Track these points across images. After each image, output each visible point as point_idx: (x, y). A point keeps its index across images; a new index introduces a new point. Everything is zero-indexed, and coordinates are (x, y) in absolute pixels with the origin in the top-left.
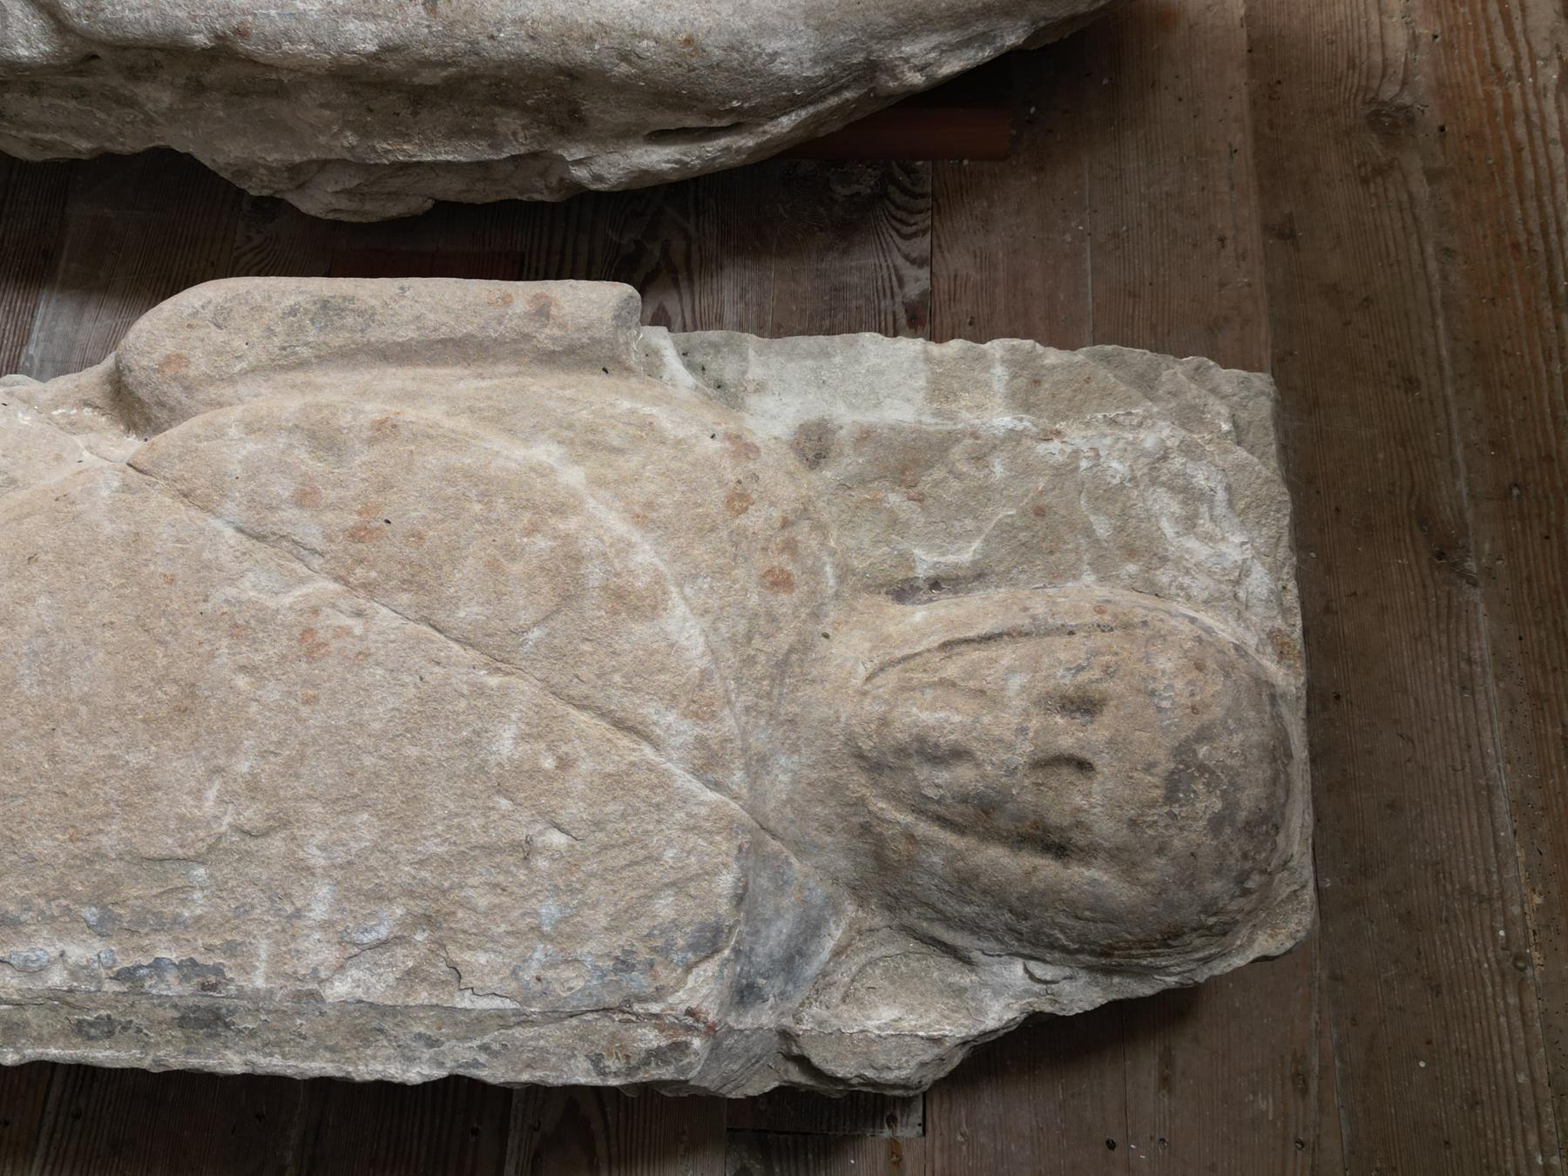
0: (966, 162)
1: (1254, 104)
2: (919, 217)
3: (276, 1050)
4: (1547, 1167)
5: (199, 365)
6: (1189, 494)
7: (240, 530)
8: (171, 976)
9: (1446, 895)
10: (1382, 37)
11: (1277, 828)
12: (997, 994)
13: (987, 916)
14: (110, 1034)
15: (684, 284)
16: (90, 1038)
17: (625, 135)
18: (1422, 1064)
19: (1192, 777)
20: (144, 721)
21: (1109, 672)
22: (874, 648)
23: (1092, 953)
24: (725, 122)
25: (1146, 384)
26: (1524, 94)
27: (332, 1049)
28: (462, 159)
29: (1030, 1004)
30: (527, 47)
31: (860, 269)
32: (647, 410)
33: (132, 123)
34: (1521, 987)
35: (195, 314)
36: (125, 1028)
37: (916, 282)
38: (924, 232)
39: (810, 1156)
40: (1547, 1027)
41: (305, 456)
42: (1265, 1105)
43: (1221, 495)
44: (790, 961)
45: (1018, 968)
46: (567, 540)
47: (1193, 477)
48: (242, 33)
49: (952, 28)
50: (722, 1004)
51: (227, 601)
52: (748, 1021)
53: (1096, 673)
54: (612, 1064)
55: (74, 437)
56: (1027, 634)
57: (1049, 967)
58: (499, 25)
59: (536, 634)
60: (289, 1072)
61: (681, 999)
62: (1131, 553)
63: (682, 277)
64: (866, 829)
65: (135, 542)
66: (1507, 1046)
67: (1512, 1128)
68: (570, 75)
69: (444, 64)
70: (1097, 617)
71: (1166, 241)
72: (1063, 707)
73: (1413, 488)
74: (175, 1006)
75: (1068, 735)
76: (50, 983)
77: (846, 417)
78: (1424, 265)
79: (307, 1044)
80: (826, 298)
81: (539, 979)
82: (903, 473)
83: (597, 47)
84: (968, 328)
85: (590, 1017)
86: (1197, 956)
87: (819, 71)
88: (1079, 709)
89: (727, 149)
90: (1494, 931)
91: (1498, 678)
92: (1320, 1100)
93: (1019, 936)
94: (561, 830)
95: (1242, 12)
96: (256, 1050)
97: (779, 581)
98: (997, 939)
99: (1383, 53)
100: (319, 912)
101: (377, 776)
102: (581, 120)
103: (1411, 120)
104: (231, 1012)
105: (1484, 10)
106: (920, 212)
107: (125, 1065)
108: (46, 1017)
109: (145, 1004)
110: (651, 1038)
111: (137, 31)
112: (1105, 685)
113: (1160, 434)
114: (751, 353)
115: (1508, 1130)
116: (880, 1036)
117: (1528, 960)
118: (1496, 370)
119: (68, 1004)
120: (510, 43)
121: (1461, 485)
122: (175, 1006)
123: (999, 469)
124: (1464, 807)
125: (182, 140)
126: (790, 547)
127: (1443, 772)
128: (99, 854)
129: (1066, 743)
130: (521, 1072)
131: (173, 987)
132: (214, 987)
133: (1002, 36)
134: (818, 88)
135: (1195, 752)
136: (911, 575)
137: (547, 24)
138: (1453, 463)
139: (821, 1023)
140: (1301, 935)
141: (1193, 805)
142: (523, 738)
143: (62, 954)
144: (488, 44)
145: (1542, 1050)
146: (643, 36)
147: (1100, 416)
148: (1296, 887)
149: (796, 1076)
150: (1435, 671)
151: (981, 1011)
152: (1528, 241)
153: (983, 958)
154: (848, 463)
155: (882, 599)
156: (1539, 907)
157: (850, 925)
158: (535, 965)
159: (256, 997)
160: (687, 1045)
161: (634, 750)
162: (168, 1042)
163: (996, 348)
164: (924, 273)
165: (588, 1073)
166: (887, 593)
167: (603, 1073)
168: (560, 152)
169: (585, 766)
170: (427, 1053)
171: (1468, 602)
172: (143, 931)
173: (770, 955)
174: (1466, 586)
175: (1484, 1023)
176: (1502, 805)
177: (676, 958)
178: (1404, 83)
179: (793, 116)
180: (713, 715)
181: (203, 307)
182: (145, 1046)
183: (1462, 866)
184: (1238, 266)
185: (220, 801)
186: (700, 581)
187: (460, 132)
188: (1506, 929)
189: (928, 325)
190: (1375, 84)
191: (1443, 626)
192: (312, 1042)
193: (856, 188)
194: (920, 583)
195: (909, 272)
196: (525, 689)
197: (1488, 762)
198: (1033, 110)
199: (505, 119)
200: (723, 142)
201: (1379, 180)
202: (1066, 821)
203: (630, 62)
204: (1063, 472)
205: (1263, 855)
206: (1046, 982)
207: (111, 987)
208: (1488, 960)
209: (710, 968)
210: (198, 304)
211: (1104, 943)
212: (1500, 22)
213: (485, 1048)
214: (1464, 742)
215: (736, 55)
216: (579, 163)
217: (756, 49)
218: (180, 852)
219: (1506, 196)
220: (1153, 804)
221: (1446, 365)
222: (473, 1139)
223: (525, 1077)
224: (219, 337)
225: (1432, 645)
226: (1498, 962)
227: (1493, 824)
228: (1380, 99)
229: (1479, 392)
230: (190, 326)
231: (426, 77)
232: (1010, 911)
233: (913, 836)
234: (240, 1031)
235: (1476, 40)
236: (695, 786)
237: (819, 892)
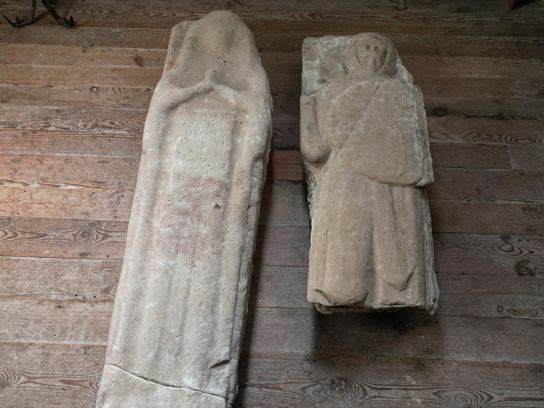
5: (320, 145)
6: (328, 44)
21: (363, 44)
22: (359, 70)
32: (324, 92)
46: (350, 95)
53: (363, 46)
59: (365, 97)
65: (354, 143)
70: (353, 48)
77: (318, 78)
93: (394, 62)
100: (407, 119)
110: (416, 89)
113: (319, 46)
123: (326, 62)
128: (403, 142)
129: (373, 49)
131: (419, 135)
142: (381, 98)
154: (326, 77)
163: (304, 62)
169: (384, 92)
185: (393, 130)
196: (373, 98)
204: (326, 55)
207: (420, 142)
224: (314, 142)
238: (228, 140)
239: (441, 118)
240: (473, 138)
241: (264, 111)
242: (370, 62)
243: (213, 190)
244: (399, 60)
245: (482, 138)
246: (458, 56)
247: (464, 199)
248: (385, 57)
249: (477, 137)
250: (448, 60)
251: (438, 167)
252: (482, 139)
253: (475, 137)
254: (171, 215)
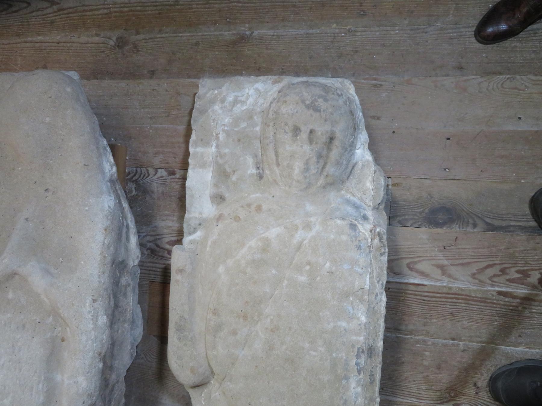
0: (127, 158)
1: (113, 79)
2: (143, 171)
3: (378, 334)
4: (398, 30)
6: (236, 101)
7: (243, 349)
8: (359, 361)
9: (333, 47)
10: (95, 43)
11: (326, 86)
12: (364, 157)
13: (346, 158)
14: (373, 375)
15: (160, 237)
16: (374, 380)
17: (127, 249)
18: (375, 56)
19: (315, 105)
20: (295, 371)
21: (286, 124)
23: (355, 132)
24: (125, 222)
25: (203, 112)
26: (115, 8)
27: (378, 320)
28: (132, 294)
29: (366, 149)
30: (106, 275)
31: (158, 188)
33: (118, 387)
34: (355, 31)
35: (179, 366)
36: (372, 371)
37: (162, 172)
38: (147, 170)
39: (396, 206)
40: (366, 27)
41: (222, 334)
42: (384, 94)
43: (236, 94)
44: (357, 207)
45: (357, 151)
47: (230, 101)
48: (100, 354)
49: (102, 158)
50: (368, 224)
51: (263, 351)
52: (371, 218)
54: (383, 250)
55: (212, 397)
56: (275, 144)
57: (358, 143)
58: (100, 282)
60: (383, 330)
61: (368, 234)
62: (251, 118)
63: (158, 237)
64: (324, 187)
66: (370, 36)
67: (390, 37)
68: (113, 263)
69: (110, 298)
71: (153, 105)
72: (295, 136)
73: (226, 45)
74: (367, 359)
75: (304, 136)
76: (361, 391)
78: (164, 37)
79: (376, 325)
80: (166, 197)
81: (362, 269)
82: (227, 176)
83: (107, 255)
84: (176, 159)
85: (371, 256)
86: (355, 107)
87: (112, 195)
88: (296, 132)
89: (131, 221)
90: (342, 36)
91: (278, 29)
92: (383, 81)
94: (326, 263)
95: (85, 81)
96: (378, 339)
97: (259, 209)
98: (351, 156)
99: (100, 43)
101: (311, 311)
102: (123, 261)
103: (121, 38)
104: (369, 345)
105: (89, 16)
106: (141, 171)
107: (380, 371)
108: (369, 392)
109: (366, 367)
110: (376, 241)
111: (98, 384)
112: (290, 125)
114: (190, 216)
115: (390, 38)
116: (374, 186)
117: (349, 29)
118: (194, 22)
119: (366, 386)
120: (105, 279)
121: (226, 33)
122: (367, 359)
123: (227, 151)
124: (311, 41)
125: (123, 372)
126: (249, 205)
127: (302, 45)
130: (384, 273)
131: (363, 360)
132: (363, 350)
133: (104, 145)
134: (116, 196)
135: (308, 104)
136: (256, 174)
137: (100, 269)
138: (220, 35)
139: (371, 200)
140: (350, 82)
141: (321, 105)
143: (354, 388)
144: (105, 285)
145: (371, 28)
146: (104, 243)
147: (213, 124)
148: (338, 83)
149: (382, 207)
150: (276, 44)
151: (368, 161)
152: (158, 10)
153: (355, 160)
154: (223, 190)
155: (262, 181)
156: (337, 25)
157: (347, 192)
158: (359, 270)
159: (367, 339)
160: (378, 232)
161: (305, 245)
162: (375, 360)
163: (191, 150)
164: (159, 170)
165: (385, 257)
166: (260, 181)
167: (385, 253)
168: (131, 268)
170: (379, 296)
171: (258, 34)
172: (349, 368)
173: (356, 212)
174: (254, 34)
175: (365, 41)
176: (311, 31)
177: (358, 234)
178: (110, 39)
179: (123, 203)
180: (296, 225)
181: (177, 363)
182: (377, 366)
183: (326, 42)
184: (161, 86)
186: (259, 229)
187: (125, 295)
188: (342, 33)
189: (175, 170)
190: (109, 46)
191: (264, 41)
192: (376, 325)
193: (133, 189)
194: (258, 172)
195: (159, 174)
197: (300, 33)
198: (112, 139)
199: (122, 282)
200: (129, 222)
201: (138, 47)
202: (325, 137)
203: (111, 246)
204: (228, 134)
205: (333, 90)
206: (361, 145)
208: (350, 38)
209: (360, 227)
210: (176, 365)
211: (353, 130)
212: (93, 12)
213: (378, 282)
214: (296, 39)
215: (109, 217)
216: (134, 262)
217: (108, 211)
218: (329, 361)
219: (145, 15)
220: (320, 115)
221: (192, 34)
222: (390, 290)
223: (385, 272)
225: (268, 45)
226: (350, 36)
227: (316, 34)
228: (114, 45)
229: (200, 27)
230: (182, 367)
231: (112, 303)
232: (345, 152)
233: (326, 175)
234: (373, 343)
235: (98, 18)
236: (314, 230)
237: (340, 200)
238: (39, 383)
239: (440, 231)
240: (490, 278)
241: (91, 326)
242: (298, 166)
244: (363, 137)
245: (508, 277)
246: (500, 73)
247: (450, 401)
248: (329, 149)
249: (499, 276)
250: (480, 83)
251: (415, 335)
252: (508, 280)
253: (495, 276)
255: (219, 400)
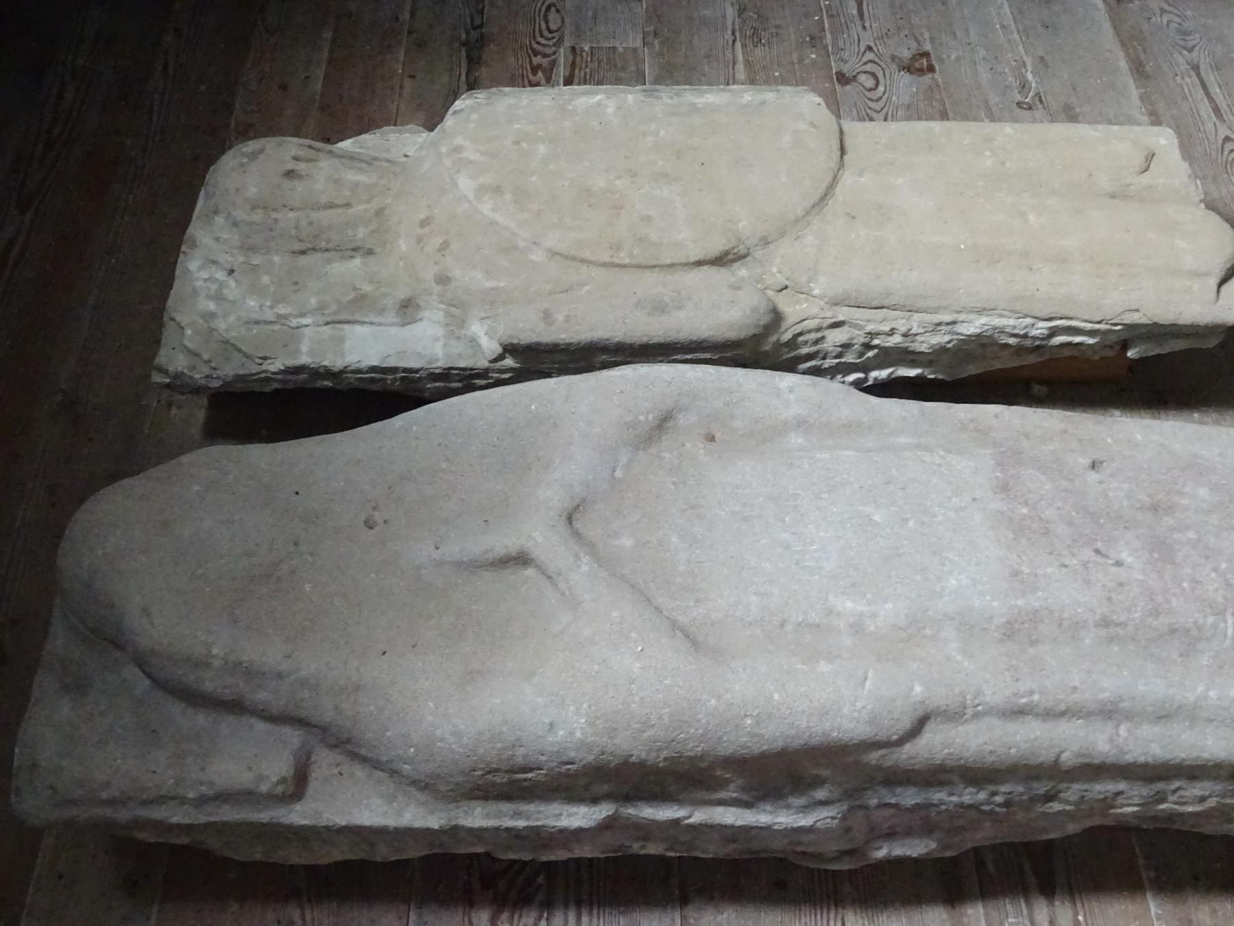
6: (218, 297)
243: (1043, 478)
254: (1185, 585)
255: (783, 257)
